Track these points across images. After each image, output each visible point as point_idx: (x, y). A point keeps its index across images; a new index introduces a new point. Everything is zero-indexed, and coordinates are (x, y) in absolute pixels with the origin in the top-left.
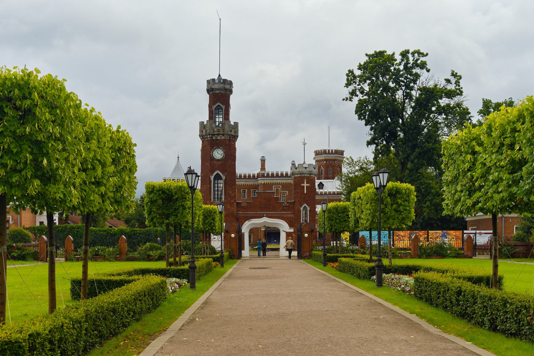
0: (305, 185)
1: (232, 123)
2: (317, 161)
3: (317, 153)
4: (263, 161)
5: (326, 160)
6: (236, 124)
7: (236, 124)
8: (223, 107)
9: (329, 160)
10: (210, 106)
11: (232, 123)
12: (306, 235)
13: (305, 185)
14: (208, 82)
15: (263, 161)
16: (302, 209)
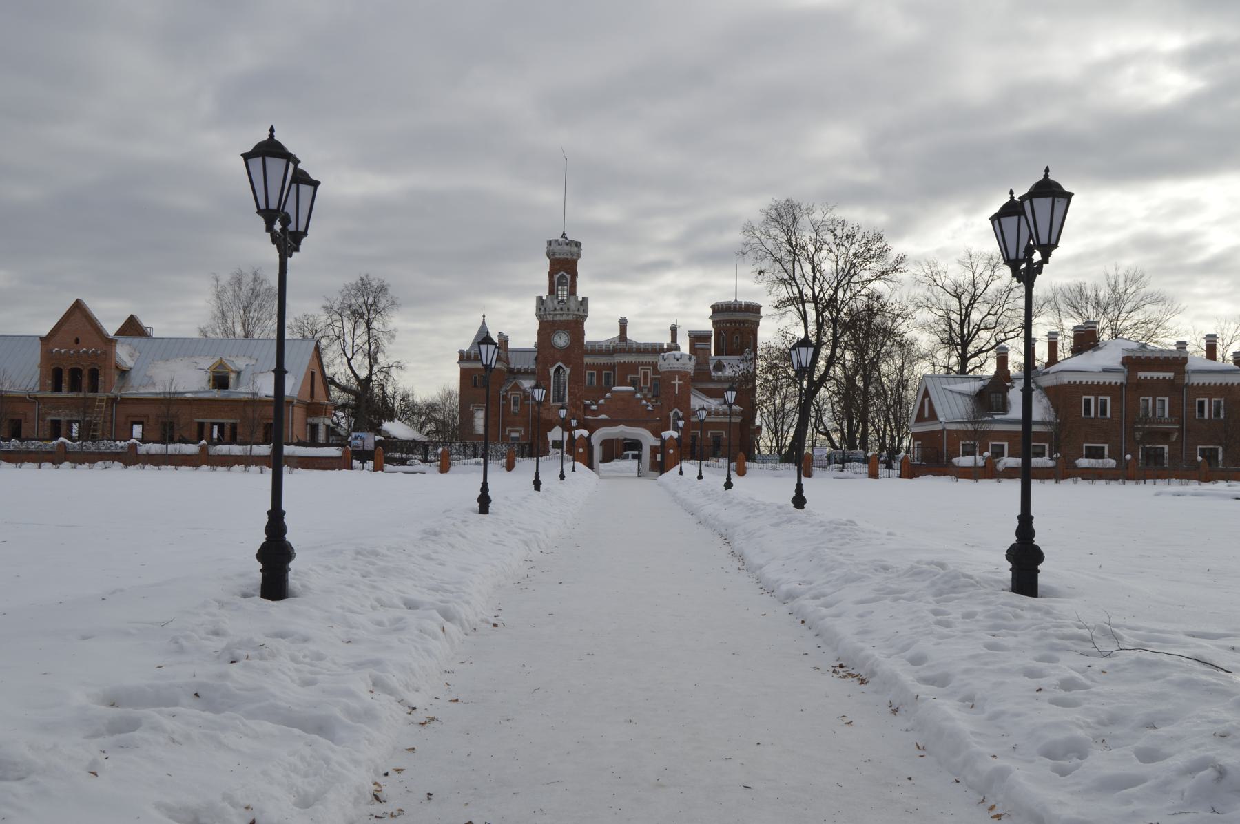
0: (677, 382)
1: (580, 297)
2: (714, 323)
3: (717, 309)
4: (623, 324)
5: (730, 322)
6: (585, 300)
7: (585, 300)
8: (569, 277)
9: (735, 322)
10: (551, 275)
11: (580, 297)
12: (671, 451)
13: (677, 382)
14: (550, 243)
15: (623, 324)
16: (672, 414)
